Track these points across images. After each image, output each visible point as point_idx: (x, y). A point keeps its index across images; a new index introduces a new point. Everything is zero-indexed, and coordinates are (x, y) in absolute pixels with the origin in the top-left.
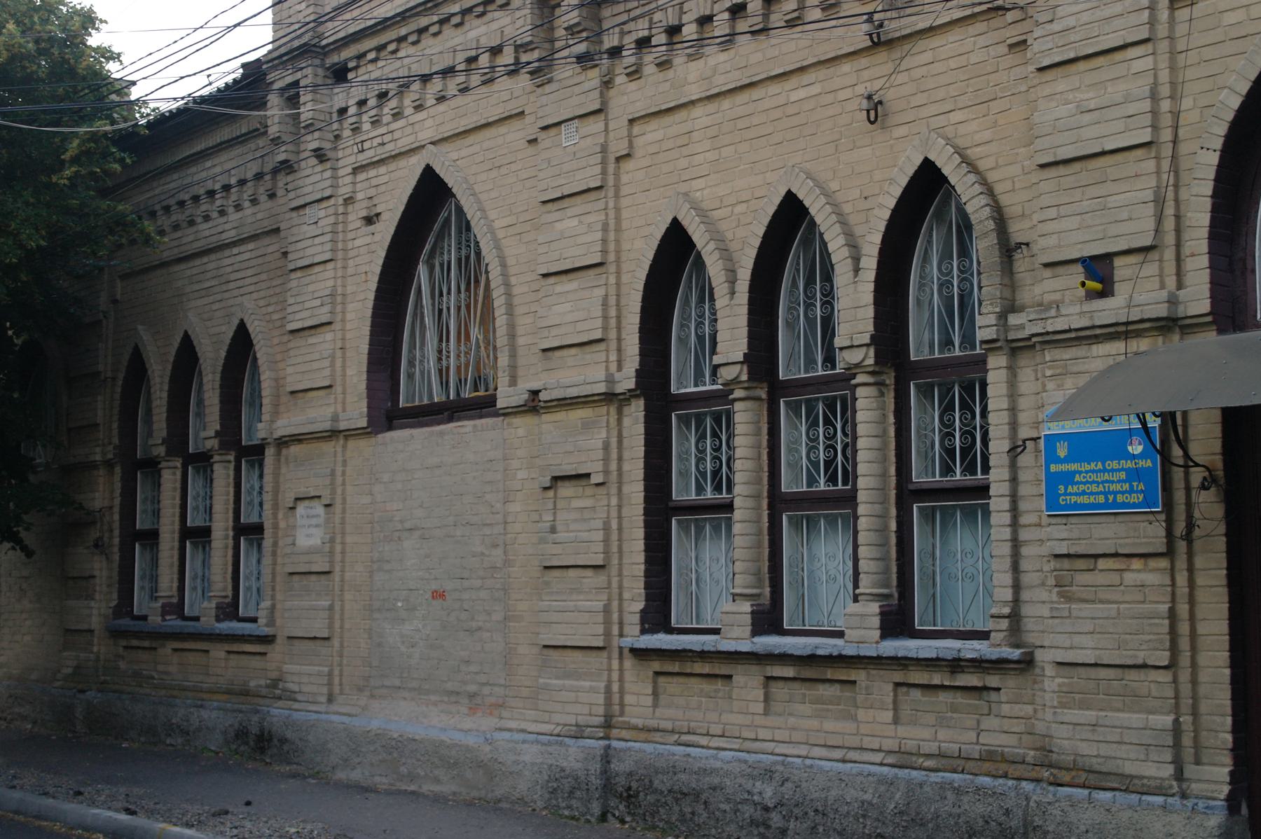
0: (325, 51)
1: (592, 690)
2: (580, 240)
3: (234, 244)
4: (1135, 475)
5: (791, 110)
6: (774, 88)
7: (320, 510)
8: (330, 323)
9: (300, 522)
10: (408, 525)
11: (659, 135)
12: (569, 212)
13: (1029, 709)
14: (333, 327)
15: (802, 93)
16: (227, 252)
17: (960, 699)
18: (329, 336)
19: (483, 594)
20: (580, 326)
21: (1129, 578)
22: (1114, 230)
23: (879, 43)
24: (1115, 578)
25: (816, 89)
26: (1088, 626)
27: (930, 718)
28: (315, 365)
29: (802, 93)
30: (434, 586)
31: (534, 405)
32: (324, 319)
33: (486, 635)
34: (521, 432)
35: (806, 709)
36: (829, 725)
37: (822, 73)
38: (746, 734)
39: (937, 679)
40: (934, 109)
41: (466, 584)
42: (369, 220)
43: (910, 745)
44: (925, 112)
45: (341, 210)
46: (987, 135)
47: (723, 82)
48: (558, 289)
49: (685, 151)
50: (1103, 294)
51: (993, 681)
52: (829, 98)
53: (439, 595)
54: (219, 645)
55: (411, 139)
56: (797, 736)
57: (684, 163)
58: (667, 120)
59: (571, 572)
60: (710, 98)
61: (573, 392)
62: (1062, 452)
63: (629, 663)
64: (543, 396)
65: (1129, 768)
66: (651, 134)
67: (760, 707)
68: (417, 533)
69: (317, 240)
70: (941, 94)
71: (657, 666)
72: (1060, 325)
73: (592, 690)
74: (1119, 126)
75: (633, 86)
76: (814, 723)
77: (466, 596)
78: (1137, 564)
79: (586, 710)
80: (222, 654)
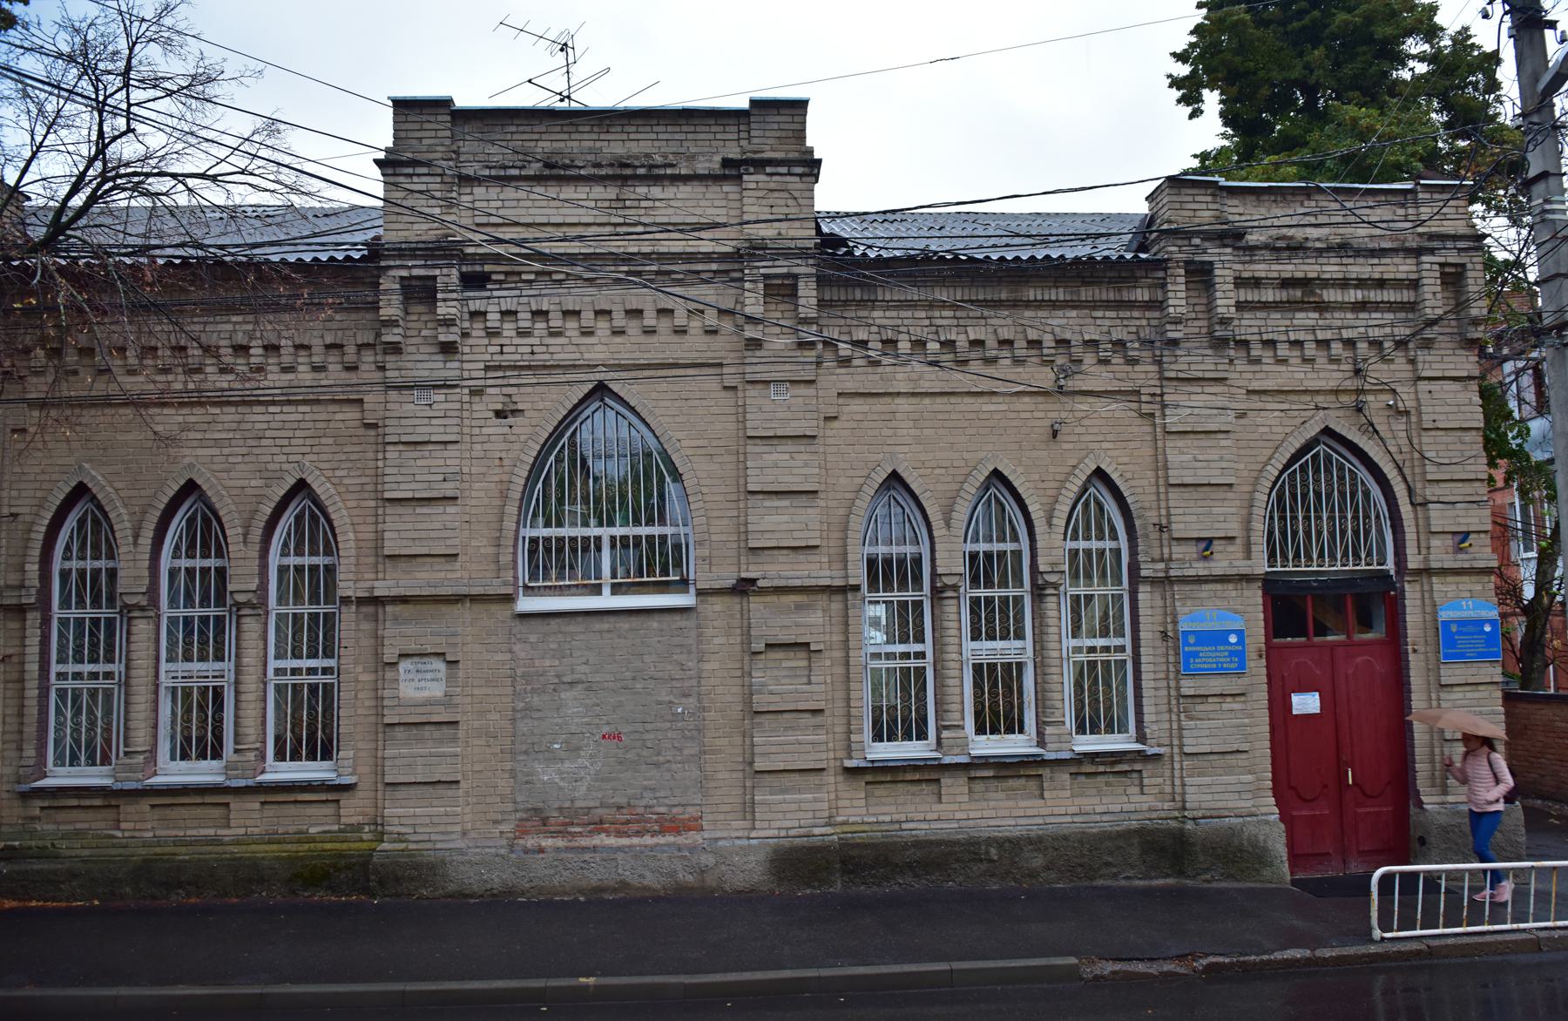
0: (464, 258)
1: (815, 800)
2: (795, 471)
3: (274, 403)
4: (1232, 653)
5: (982, 416)
6: (968, 400)
7: (441, 666)
9: (402, 676)
11: (866, 408)
12: (779, 448)
13: (1160, 780)
15: (992, 407)
17: (1111, 779)
18: (451, 509)
20: (795, 534)
21: (1225, 706)
22: (1217, 525)
23: (1061, 390)
24: (1217, 707)
25: (1003, 407)
26: (1207, 732)
27: (1094, 791)
28: (433, 534)
29: (992, 407)
30: (606, 729)
31: (744, 588)
32: (449, 494)
33: (674, 767)
34: (718, 608)
35: (1001, 795)
36: (1023, 804)
37: (1008, 399)
38: (959, 815)
39: (1101, 769)
40: (1090, 438)
41: (649, 727)
42: (499, 414)
43: (1088, 809)
44: (1083, 438)
45: (466, 398)
46: (1126, 460)
47: (926, 386)
48: (767, 503)
49: (889, 424)
50: (1205, 558)
51: (1137, 767)
52: (1013, 415)
55: (577, 356)
56: (1001, 813)
57: (890, 432)
58: (870, 400)
59: (786, 716)
60: (914, 394)
61: (798, 583)
62: (1192, 640)
63: (840, 778)
64: (760, 583)
65: (1230, 805)
66: (857, 406)
67: (966, 798)
69: (434, 421)
70: (1095, 430)
71: (869, 778)
72: (1192, 572)
73: (815, 800)
74: (1218, 472)
75: (843, 371)
76: (1011, 803)
77: (647, 736)
78: (1229, 699)
79: (810, 815)
80: (257, 806)
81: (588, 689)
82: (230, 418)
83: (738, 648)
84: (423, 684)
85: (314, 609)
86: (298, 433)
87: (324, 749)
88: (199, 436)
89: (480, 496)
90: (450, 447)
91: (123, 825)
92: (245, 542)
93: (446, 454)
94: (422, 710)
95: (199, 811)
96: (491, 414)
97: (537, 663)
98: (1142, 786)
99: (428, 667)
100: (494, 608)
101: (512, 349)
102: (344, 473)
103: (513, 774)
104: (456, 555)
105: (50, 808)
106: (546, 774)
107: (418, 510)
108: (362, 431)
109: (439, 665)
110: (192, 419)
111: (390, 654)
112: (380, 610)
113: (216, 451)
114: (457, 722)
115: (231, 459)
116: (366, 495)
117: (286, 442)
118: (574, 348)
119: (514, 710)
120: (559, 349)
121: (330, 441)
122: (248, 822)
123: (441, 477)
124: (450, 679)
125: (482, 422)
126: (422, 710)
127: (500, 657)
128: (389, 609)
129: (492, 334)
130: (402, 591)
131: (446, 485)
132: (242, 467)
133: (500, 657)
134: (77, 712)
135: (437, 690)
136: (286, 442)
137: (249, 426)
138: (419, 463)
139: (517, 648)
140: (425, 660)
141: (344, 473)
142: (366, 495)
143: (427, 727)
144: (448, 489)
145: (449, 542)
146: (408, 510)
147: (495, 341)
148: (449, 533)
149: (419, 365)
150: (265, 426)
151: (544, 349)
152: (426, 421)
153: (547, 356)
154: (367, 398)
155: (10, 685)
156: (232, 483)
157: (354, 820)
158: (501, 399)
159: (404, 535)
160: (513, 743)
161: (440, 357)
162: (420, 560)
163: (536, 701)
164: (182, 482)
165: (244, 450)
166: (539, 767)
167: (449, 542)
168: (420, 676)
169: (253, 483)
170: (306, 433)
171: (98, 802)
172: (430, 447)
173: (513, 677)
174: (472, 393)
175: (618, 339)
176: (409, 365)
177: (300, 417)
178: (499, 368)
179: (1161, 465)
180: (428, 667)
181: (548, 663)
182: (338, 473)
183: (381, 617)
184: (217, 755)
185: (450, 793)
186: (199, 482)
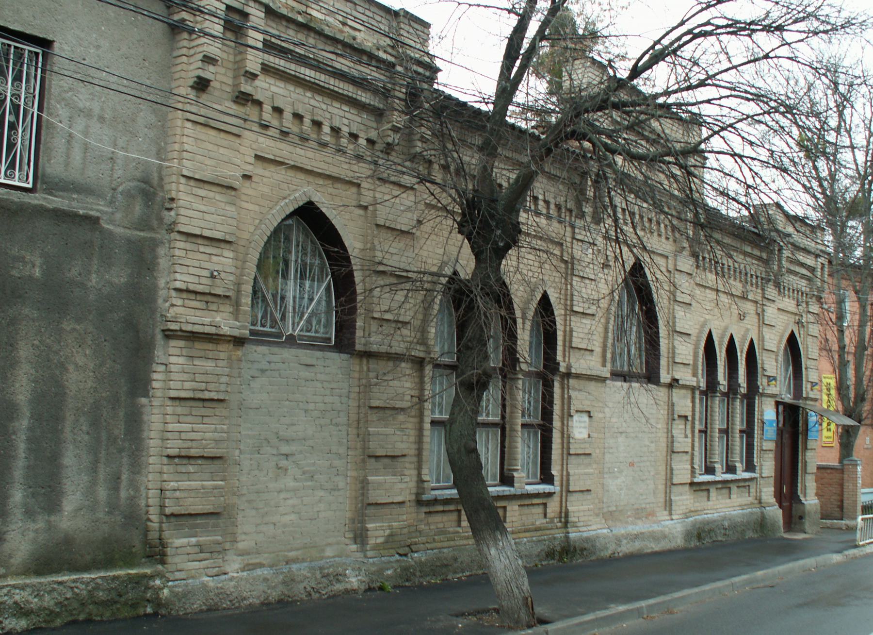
10: (620, 430)
19: (648, 464)
30: (630, 460)
54: (514, 502)
64: (680, 382)
68: (624, 435)
80: (516, 507)
83: (666, 417)
98: (749, 492)
109: (585, 418)
128: (571, 381)
143: (582, 457)
179: (762, 339)
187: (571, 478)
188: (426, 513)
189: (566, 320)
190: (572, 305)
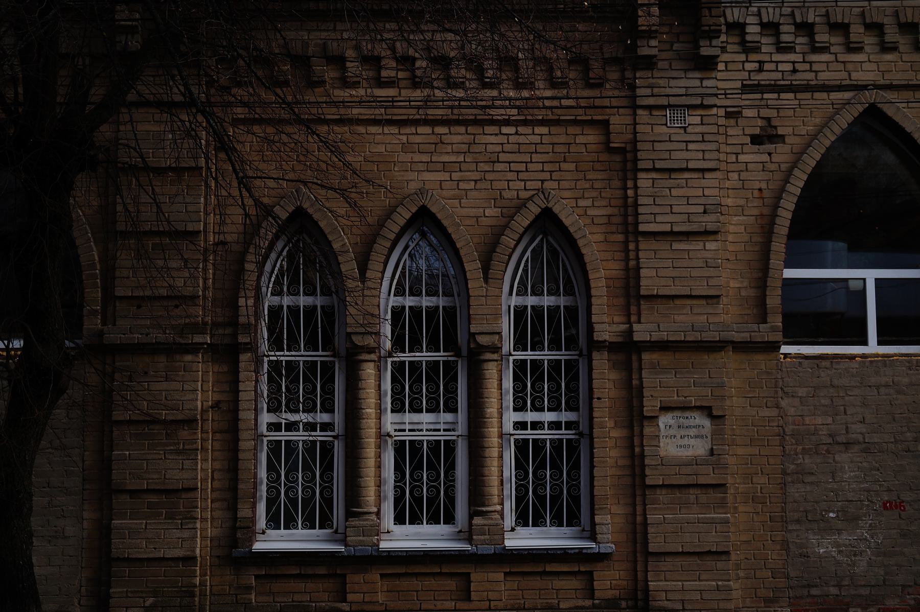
3: (507, 123)
8: (715, 233)
14: (719, 237)
16: (489, 129)
18: (711, 246)
28: (695, 273)
32: (710, 227)
42: (756, 140)
45: (722, 121)
53: (899, 505)
55: (844, 75)
68: (856, 448)
69: (691, 146)
80: (501, 576)
81: (866, 451)
82: (459, 138)
84: (686, 441)
85: (554, 355)
86: (535, 157)
87: (566, 513)
88: (425, 158)
89: (738, 228)
90: (707, 175)
91: (350, 597)
92: (486, 279)
93: (704, 183)
94: (688, 470)
95: (432, 583)
96: (748, 140)
97: (807, 420)
99: (692, 422)
100: (759, 358)
101: (772, 66)
102: (589, 203)
103: (785, 545)
104: (718, 297)
105: (266, 576)
106: (823, 547)
107: (676, 246)
108: (604, 157)
110: (418, 139)
111: (650, 406)
112: (634, 358)
113: (446, 176)
114: (723, 485)
115: (462, 185)
116: (614, 228)
117: (522, 167)
118: (841, 67)
119: (784, 473)
120: (823, 67)
121: (572, 166)
122: (491, 595)
123: (701, 209)
124: (717, 434)
125: (738, 149)
126: (688, 470)
127: (766, 413)
128: (646, 356)
129: (748, 48)
130: (664, 336)
131: (707, 218)
132: (474, 193)
133: (766, 413)
134: (292, 469)
135: (700, 448)
136: (522, 167)
137: (481, 148)
138: (675, 192)
139: (783, 403)
140: (687, 414)
141: (589, 203)
142: (614, 228)
144: (709, 222)
145: (712, 282)
146: (664, 245)
147: (753, 57)
148: (711, 272)
149: (673, 83)
150: (499, 148)
151: (807, 66)
152: (683, 146)
153: (811, 76)
154: (613, 120)
155: (218, 436)
156: (465, 212)
157: (610, 594)
158: (760, 122)
159: (662, 273)
160: (783, 510)
161: (698, 75)
162: (678, 302)
163: (808, 462)
164: (414, 210)
165: (476, 176)
166: (813, 539)
167: (712, 282)
168: (683, 432)
169: (488, 212)
170: (545, 158)
171: (322, 571)
172: (687, 175)
173: (782, 436)
174: (728, 115)
175: (889, 57)
176: (661, 82)
177: (537, 139)
178: (758, 88)
180: (692, 422)
181: (819, 420)
182: (581, 203)
183: (635, 365)
184: (450, 519)
185: (720, 565)
186: (434, 209)
187: (651, 530)
188: (257, 577)
189: (627, 251)
190: (637, 223)
